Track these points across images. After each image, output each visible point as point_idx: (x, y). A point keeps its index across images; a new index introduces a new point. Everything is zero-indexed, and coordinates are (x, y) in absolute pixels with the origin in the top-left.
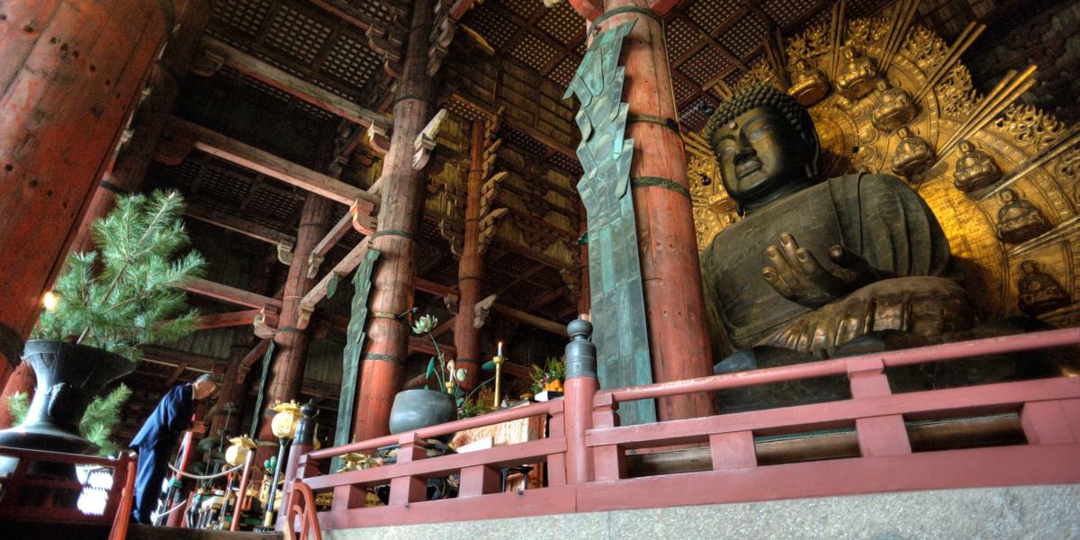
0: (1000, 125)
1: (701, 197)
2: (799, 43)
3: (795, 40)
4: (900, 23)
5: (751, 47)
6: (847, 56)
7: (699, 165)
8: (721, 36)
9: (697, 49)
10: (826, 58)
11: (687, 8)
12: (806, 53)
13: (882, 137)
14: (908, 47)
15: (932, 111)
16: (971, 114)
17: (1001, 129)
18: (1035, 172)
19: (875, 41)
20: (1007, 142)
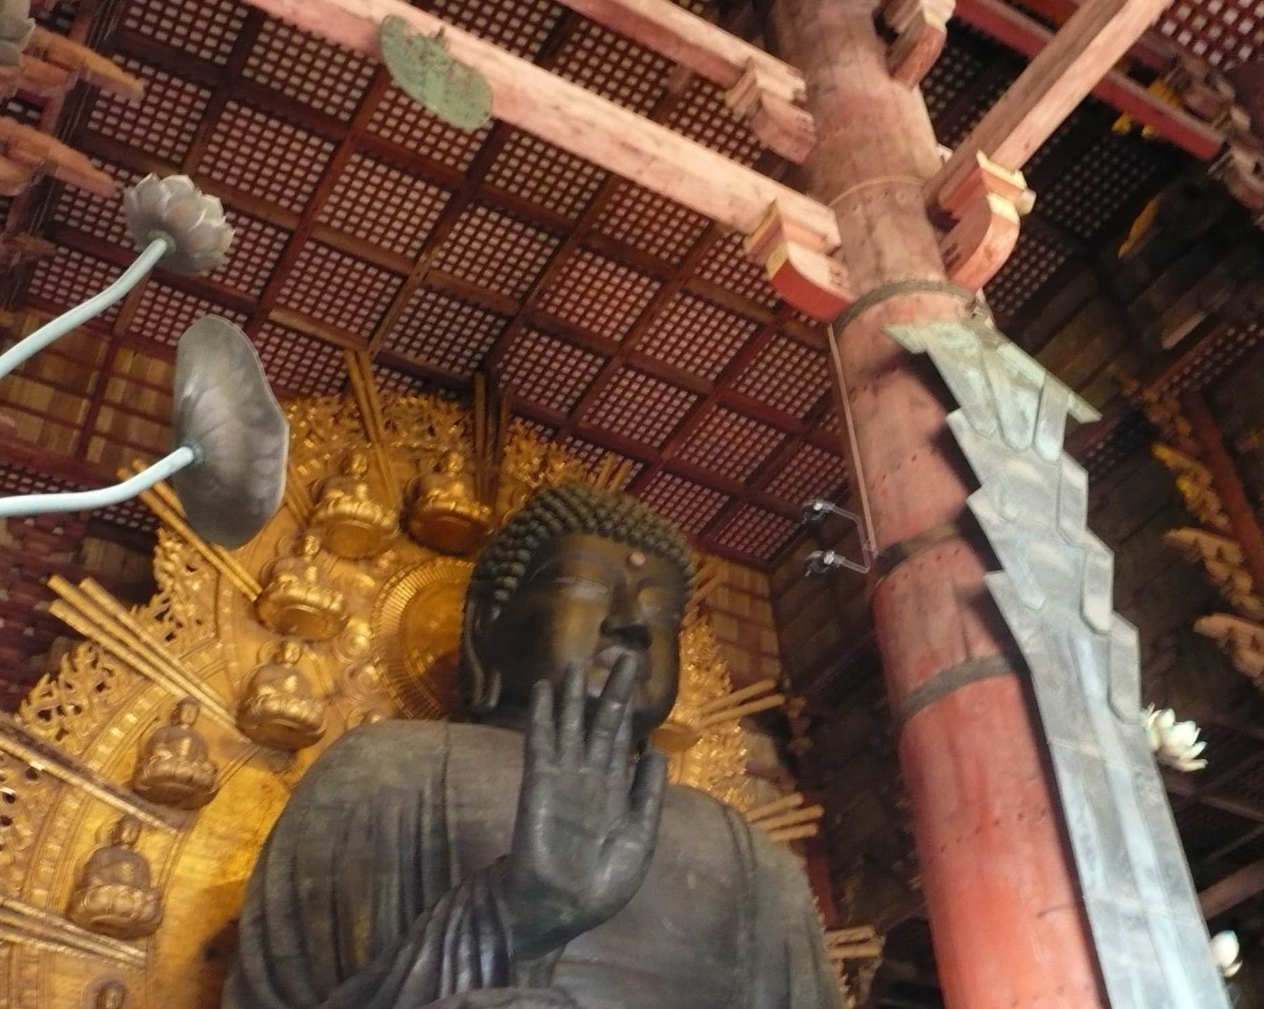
3: (527, 438)
5: (419, 351)
8: (429, 289)
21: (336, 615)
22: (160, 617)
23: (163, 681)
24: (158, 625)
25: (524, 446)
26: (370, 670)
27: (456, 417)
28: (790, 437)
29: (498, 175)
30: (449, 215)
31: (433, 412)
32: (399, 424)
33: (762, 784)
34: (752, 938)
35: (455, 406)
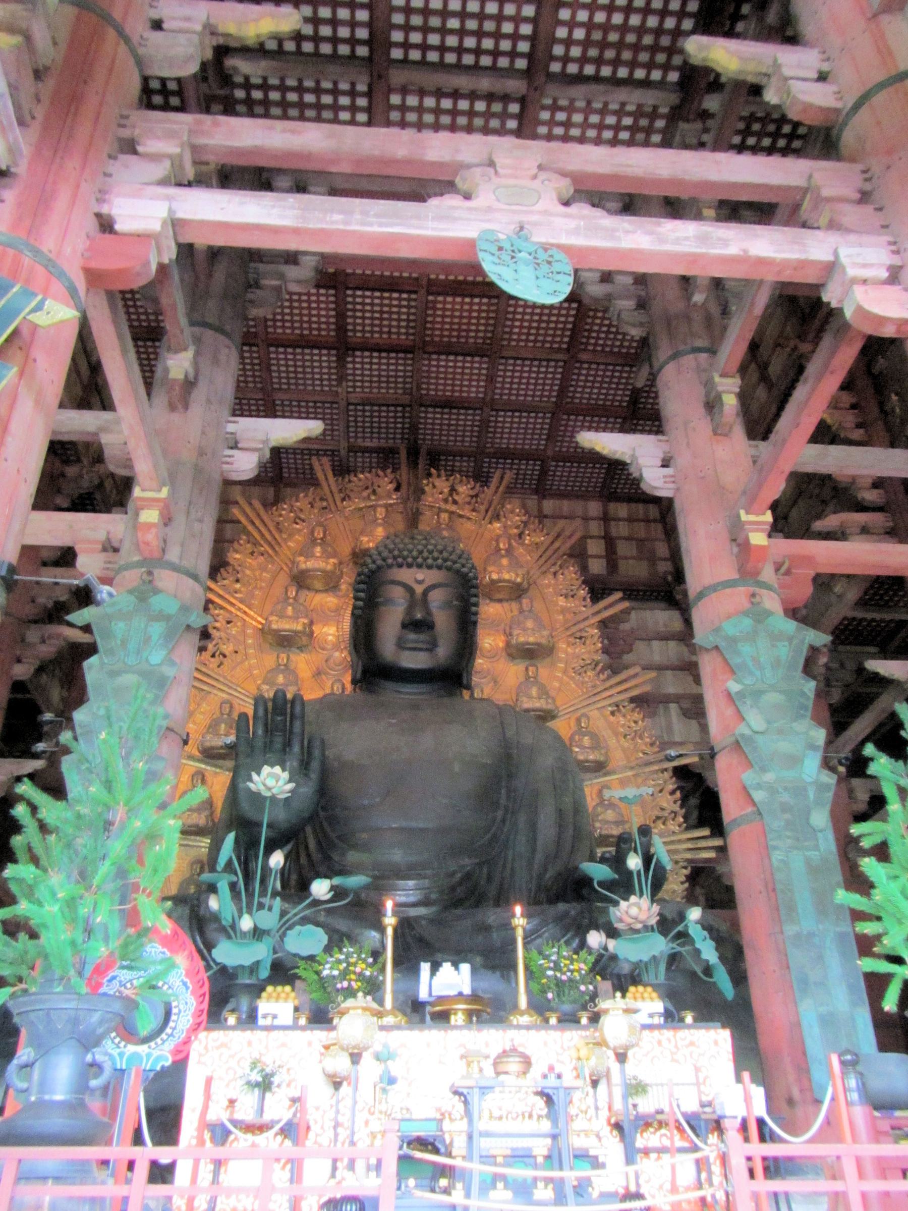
0: (613, 713)
1: (241, 601)
2: (442, 484)
3: (439, 476)
4: (557, 545)
5: (371, 438)
6: (501, 546)
7: (252, 553)
9: (317, 398)
10: (469, 525)
11: (354, 350)
12: (446, 501)
13: (502, 660)
14: (555, 574)
15: (560, 661)
16: (594, 686)
17: (612, 718)
18: (628, 777)
19: (523, 544)
20: (616, 734)
21: (303, 632)
22: (213, 656)
23: (215, 692)
24: (212, 660)
25: (437, 482)
26: (337, 654)
27: (392, 476)
28: (625, 419)
29: (354, 331)
30: (341, 361)
31: (375, 480)
32: (352, 495)
33: (672, 644)
34: (509, 791)
35: (389, 471)
